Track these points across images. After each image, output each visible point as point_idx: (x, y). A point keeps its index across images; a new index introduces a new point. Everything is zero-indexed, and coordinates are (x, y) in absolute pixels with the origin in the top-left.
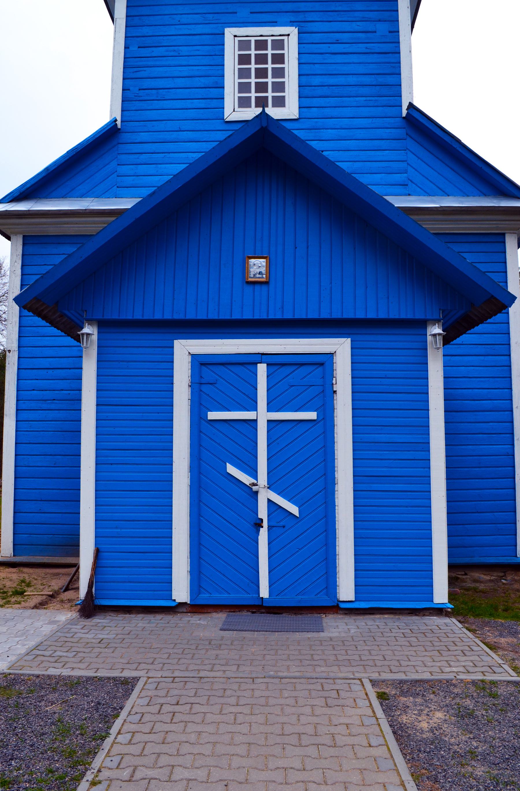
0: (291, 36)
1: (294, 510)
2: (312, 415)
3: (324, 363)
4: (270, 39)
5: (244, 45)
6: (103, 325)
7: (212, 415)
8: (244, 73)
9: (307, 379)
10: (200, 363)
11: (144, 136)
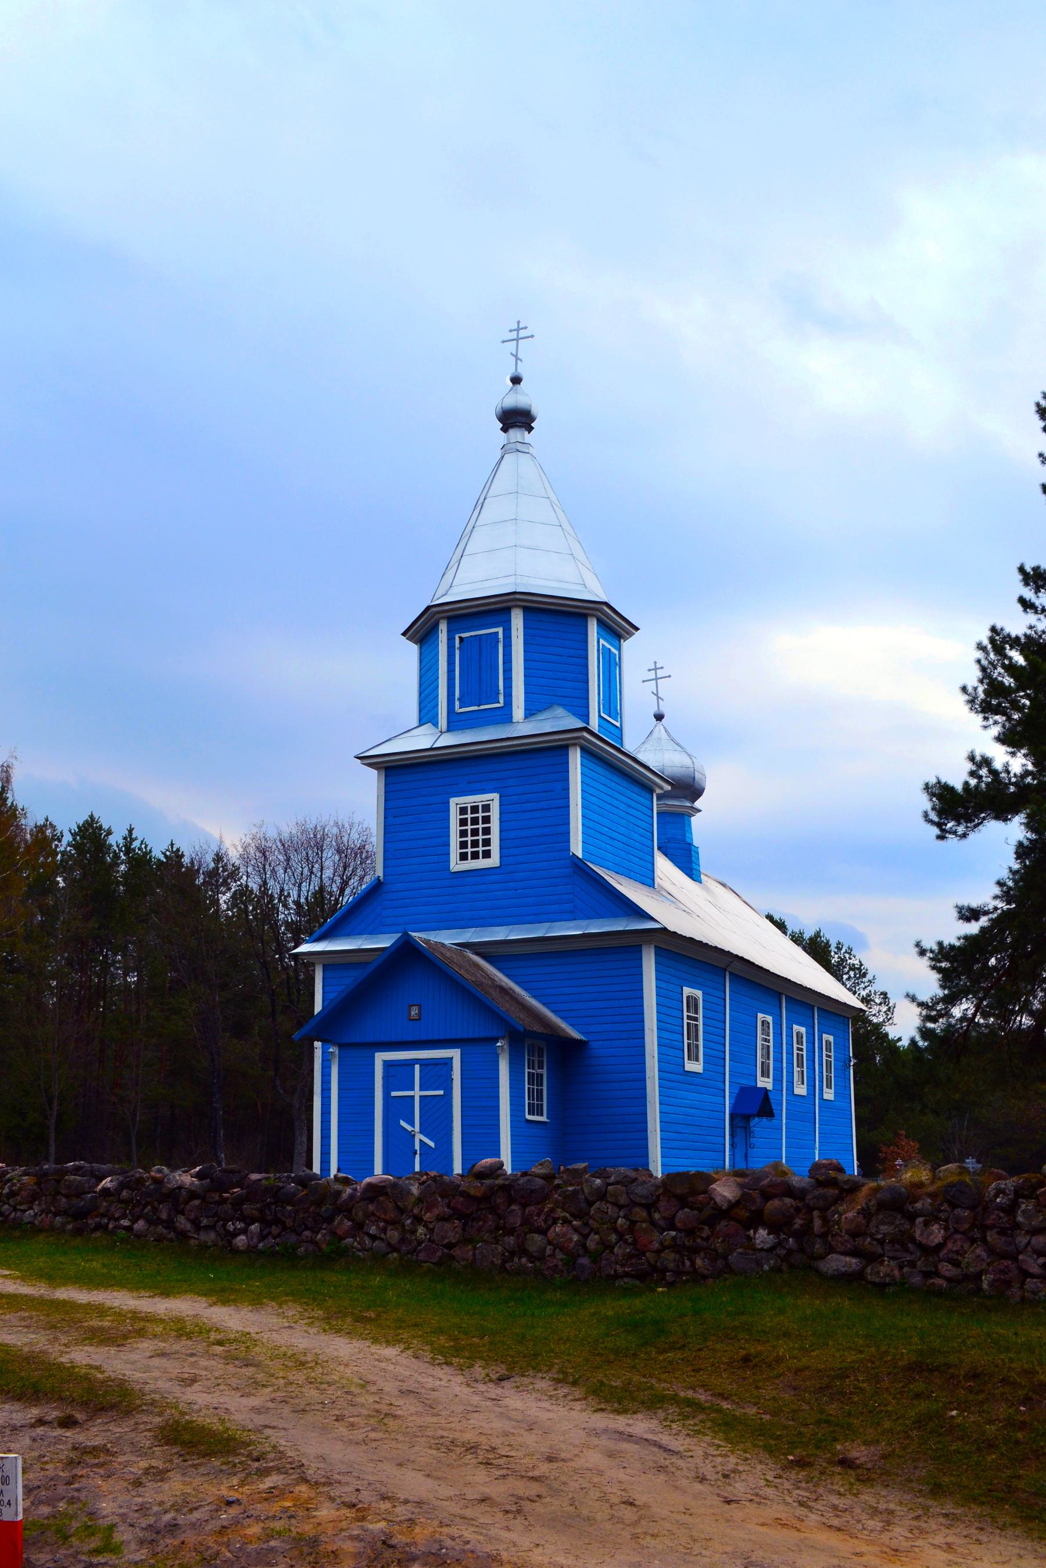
0: (493, 799)
1: (432, 1144)
2: (441, 1092)
3: (448, 1062)
4: (480, 804)
5: (463, 811)
6: (342, 1046)
7: (393, 1094)
8: (463, 834)
10: (388, 1065)
11: (398, 886)
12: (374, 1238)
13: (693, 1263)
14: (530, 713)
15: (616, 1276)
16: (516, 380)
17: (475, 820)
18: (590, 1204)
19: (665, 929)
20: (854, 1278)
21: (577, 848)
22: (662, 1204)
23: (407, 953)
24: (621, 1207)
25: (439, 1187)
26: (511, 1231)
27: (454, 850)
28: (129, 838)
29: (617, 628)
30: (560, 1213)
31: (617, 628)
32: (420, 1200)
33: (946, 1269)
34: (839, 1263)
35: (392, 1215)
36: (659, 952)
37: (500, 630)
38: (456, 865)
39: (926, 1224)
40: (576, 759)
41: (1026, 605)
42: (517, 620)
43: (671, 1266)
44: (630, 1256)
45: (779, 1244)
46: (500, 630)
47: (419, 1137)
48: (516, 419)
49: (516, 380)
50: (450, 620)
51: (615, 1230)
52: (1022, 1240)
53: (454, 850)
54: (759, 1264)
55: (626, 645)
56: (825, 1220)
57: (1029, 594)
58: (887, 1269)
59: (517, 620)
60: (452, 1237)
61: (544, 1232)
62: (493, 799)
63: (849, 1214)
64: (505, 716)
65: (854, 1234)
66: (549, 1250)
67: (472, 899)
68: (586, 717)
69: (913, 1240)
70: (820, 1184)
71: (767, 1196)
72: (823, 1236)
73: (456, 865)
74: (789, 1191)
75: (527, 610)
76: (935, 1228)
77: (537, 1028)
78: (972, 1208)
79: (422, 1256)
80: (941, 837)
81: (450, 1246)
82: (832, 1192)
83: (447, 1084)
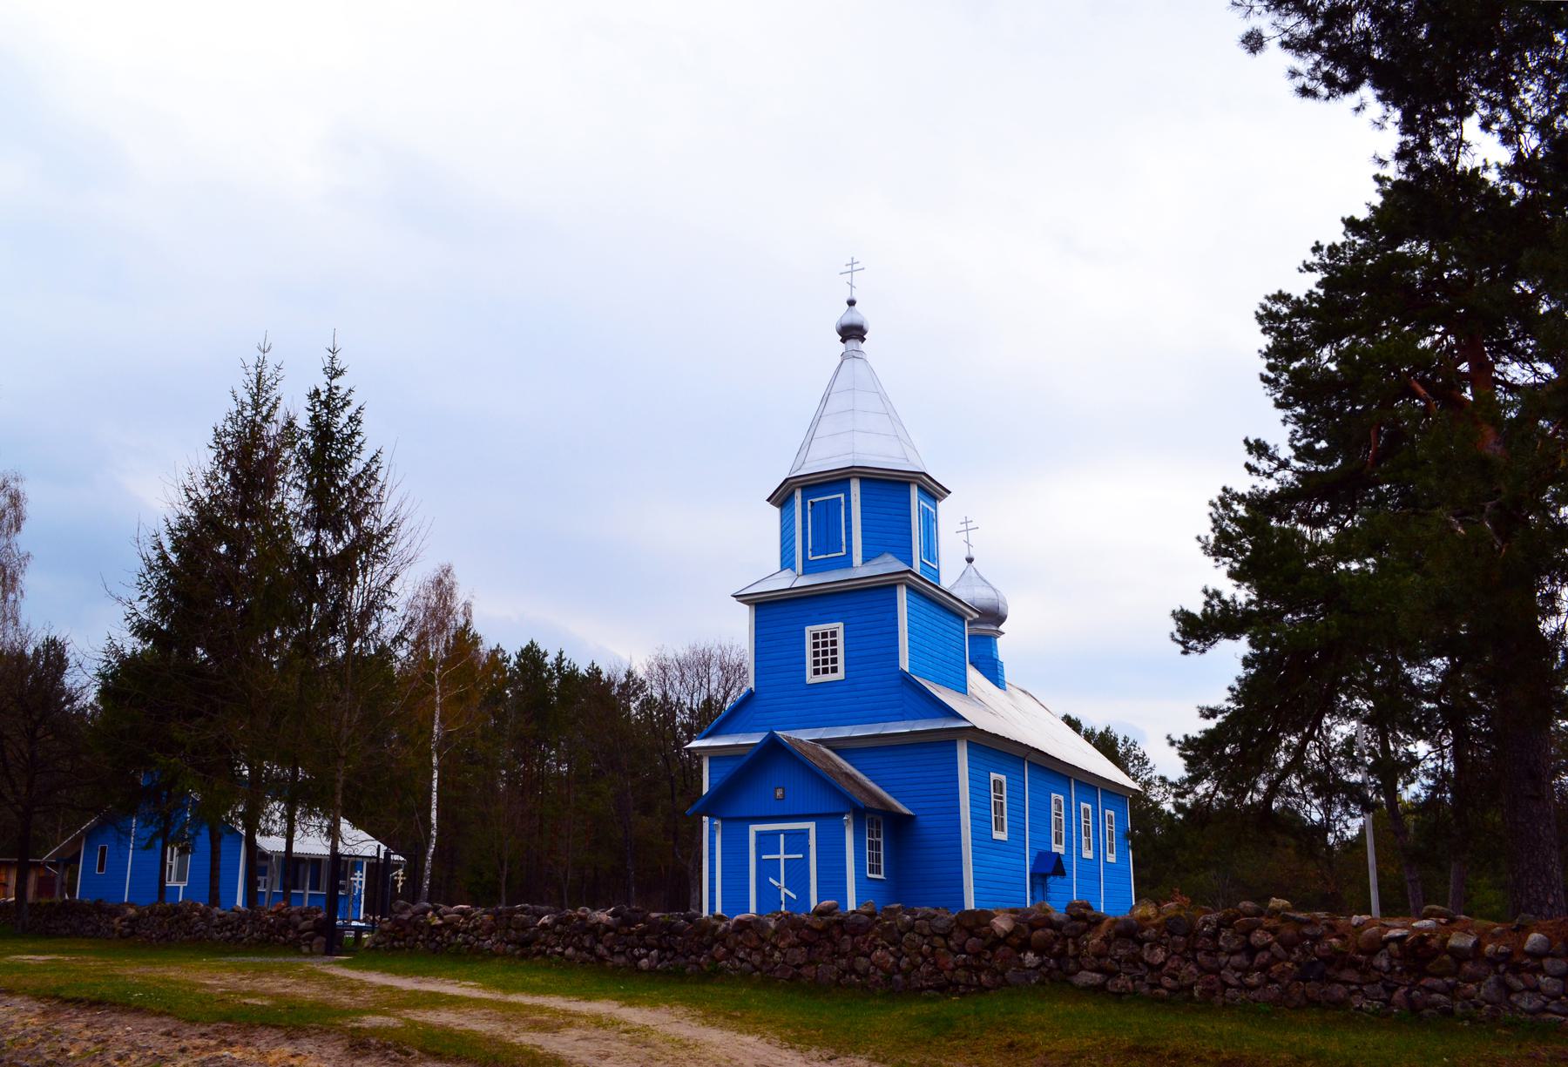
0: (839, 627)
3: (805, 832)
5: (816, 636)
6: (723, 820)
8: (816, 654)
9: (797, 841)
10: (759, 834)
12: (742, 961)
13: (979, 978)
14: (866, 559)
15: (922, 989)
16: (851, 303)
17: (825, 643)
18: (902, 934)
19: (974, 728)
20: (1097, 990)
21: (905, 664)
22: (955, 934)
23: (774, 749)
24: (925, 937)
25: (790, 923)
26: (844, 955)
27: (809, 667)
28: (560, 659)
29: (934, 492)
30: (879, 941)
31: (934, 492)
32: (776, 932)
33: (1167, 982)
34: (1087, 977)
35: (755, 943)
36: (970, 745)
37: (842, 496)
38: (811, 678)
39: (1152, 948)
40: (902, 594)
41: (1251, 469)
42: (855, 487)
43: (963, 980)
44: (932, 974)
45: (1042, 964)
46: (842, 496)
47: (784, 891)
48: (852, 333)
49: (851, 303)
50: (804, 488)
51: (921, 954)
52: (1223, 959)
53: (809, 667)
54: (1028, 979)
55: (941, 505)
56: (1077, 946)
57: (1253, 460)
58: (1122, 981)
59: (855, 487)
60: (800, 960)
61: (868, 956)
62: (839, 627)
63: (1094, 940)
64: (847, 562)
65: (1098, 956)
66: (872, 969)
67: (823, 705)
68: (910, 562)
69: (1142, 960)
70: (1073, 918)
71: (1033, 928)
72: (1075, 957)
73: (811, 678)
74: (1050, 923)
75: (862, 480)
76: (1158, 950)
77: (875, 805)
78: (1185, 936)
79: (778, 974)
80: (1185, 653)
81: (798, 966)
82: (1082, 924)
83: (805, 850)
